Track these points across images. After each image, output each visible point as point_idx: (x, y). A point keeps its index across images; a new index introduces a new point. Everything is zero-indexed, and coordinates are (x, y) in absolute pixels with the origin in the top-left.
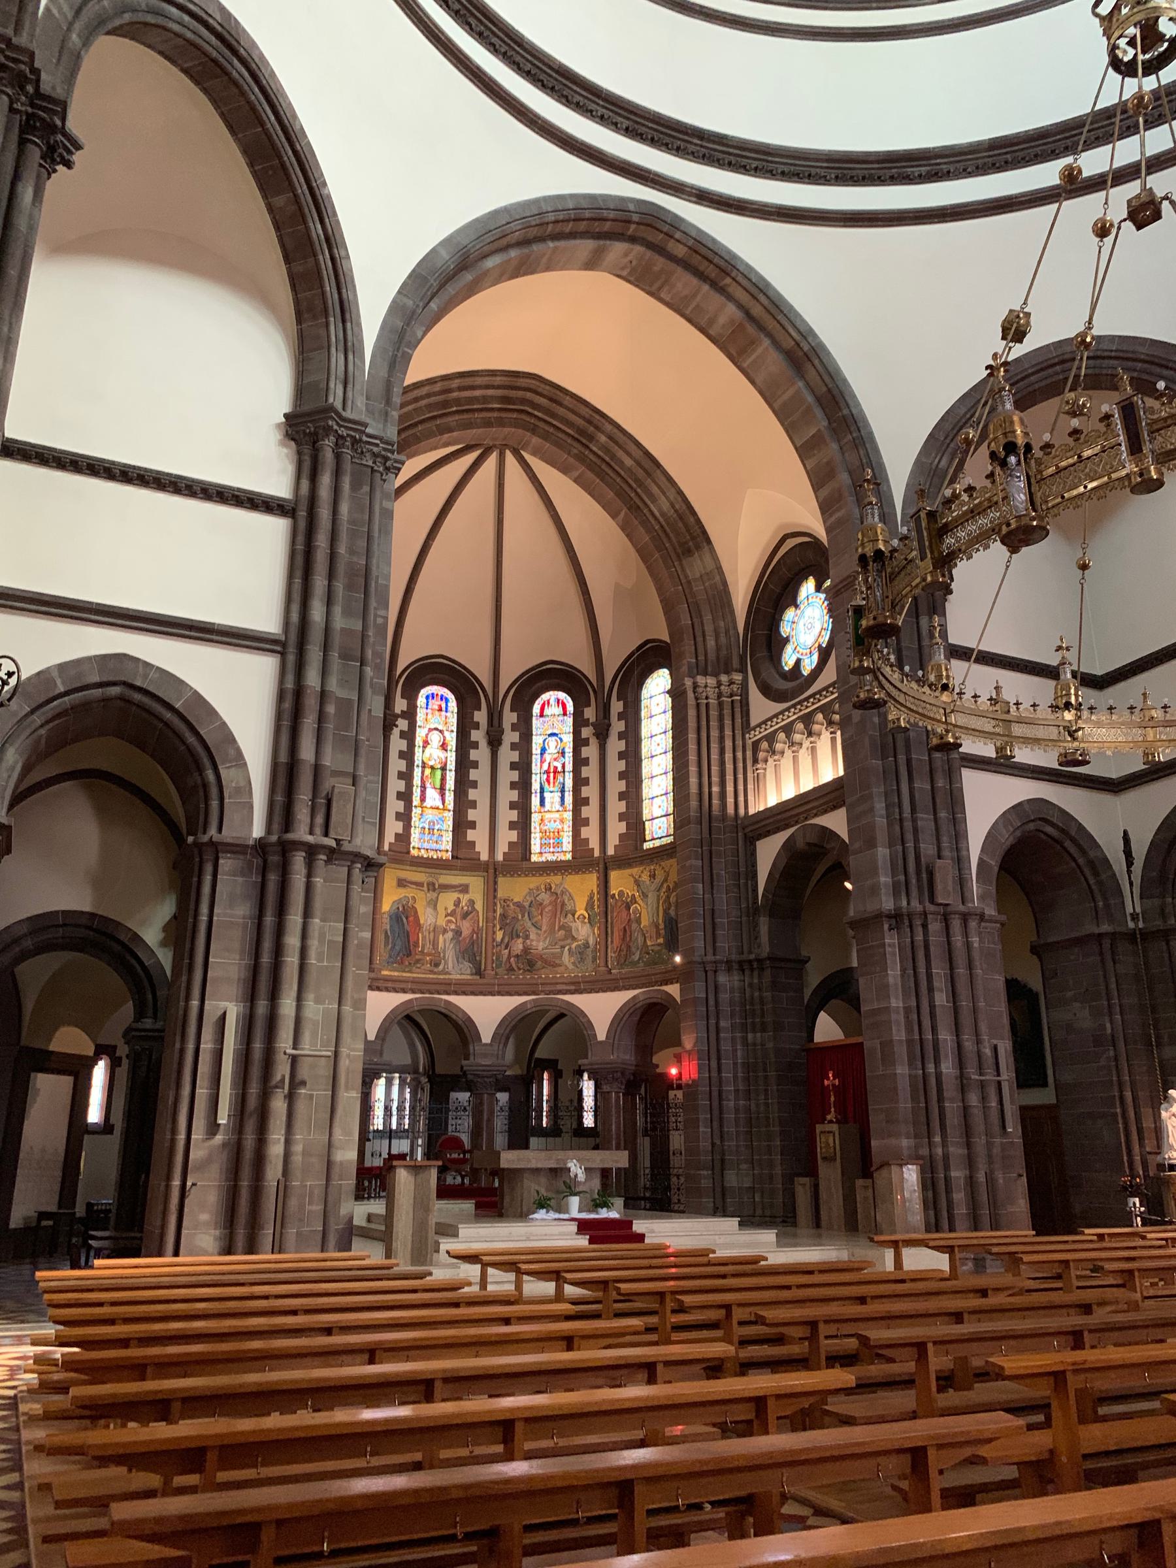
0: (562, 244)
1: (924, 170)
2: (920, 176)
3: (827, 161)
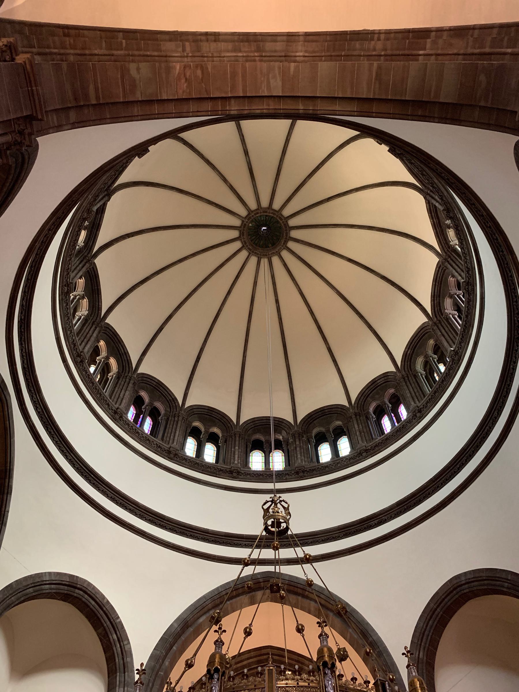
0: (234, 600)
1: (376, 521)
2: (375, 524)
3: (339, 530)
